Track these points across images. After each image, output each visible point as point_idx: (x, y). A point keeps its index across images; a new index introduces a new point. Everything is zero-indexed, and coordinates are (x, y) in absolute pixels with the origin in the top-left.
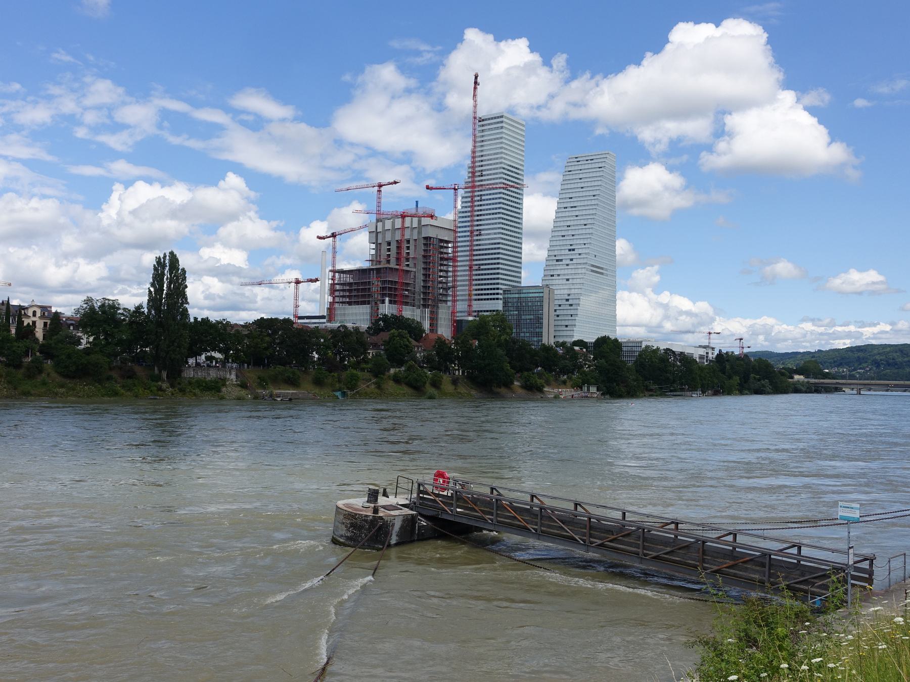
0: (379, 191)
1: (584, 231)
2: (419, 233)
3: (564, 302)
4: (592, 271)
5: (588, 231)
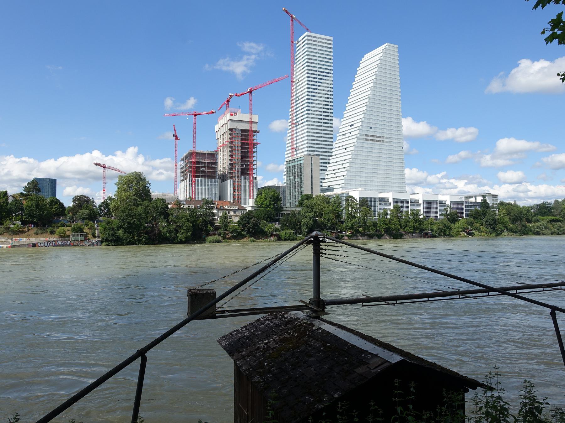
3: (341, 166)
4: (366, 139)
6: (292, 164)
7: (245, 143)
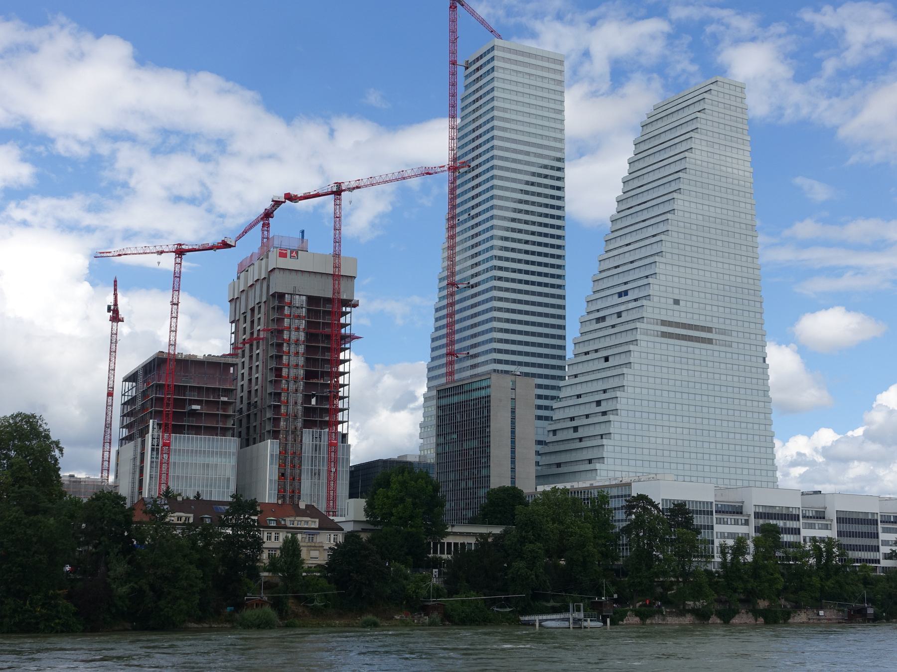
0: (266, 226)
3: (594, 409)
4: (664, 335)
6: (456, 399)
7: (317, 335)
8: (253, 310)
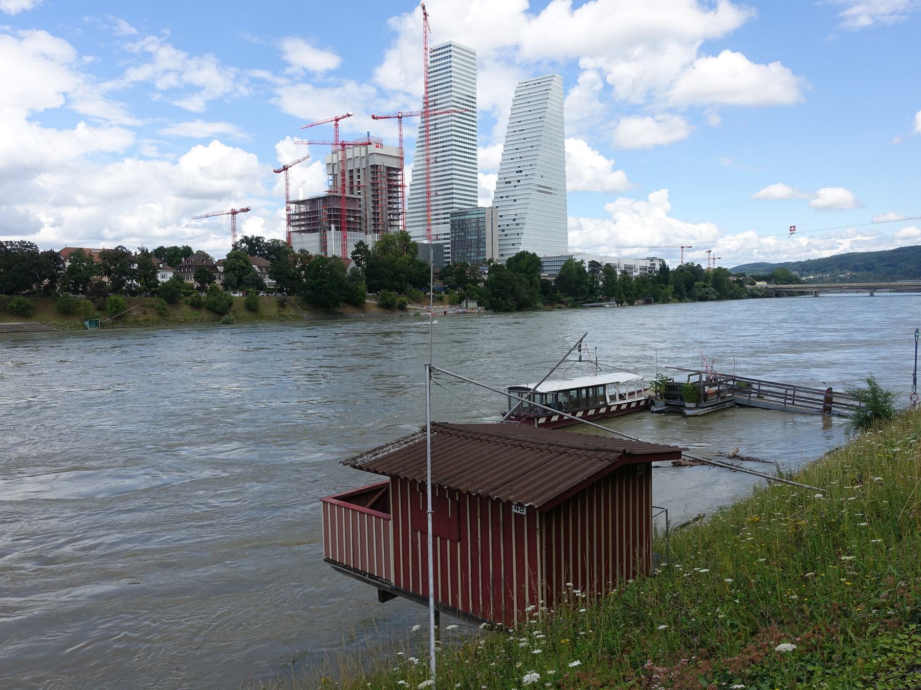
0: (336, 125)
1: (530, 153)
2: (367, 162)
3: (512, 222)
4: (539, 191)
5: (534, 153)
8: (351, 171)
